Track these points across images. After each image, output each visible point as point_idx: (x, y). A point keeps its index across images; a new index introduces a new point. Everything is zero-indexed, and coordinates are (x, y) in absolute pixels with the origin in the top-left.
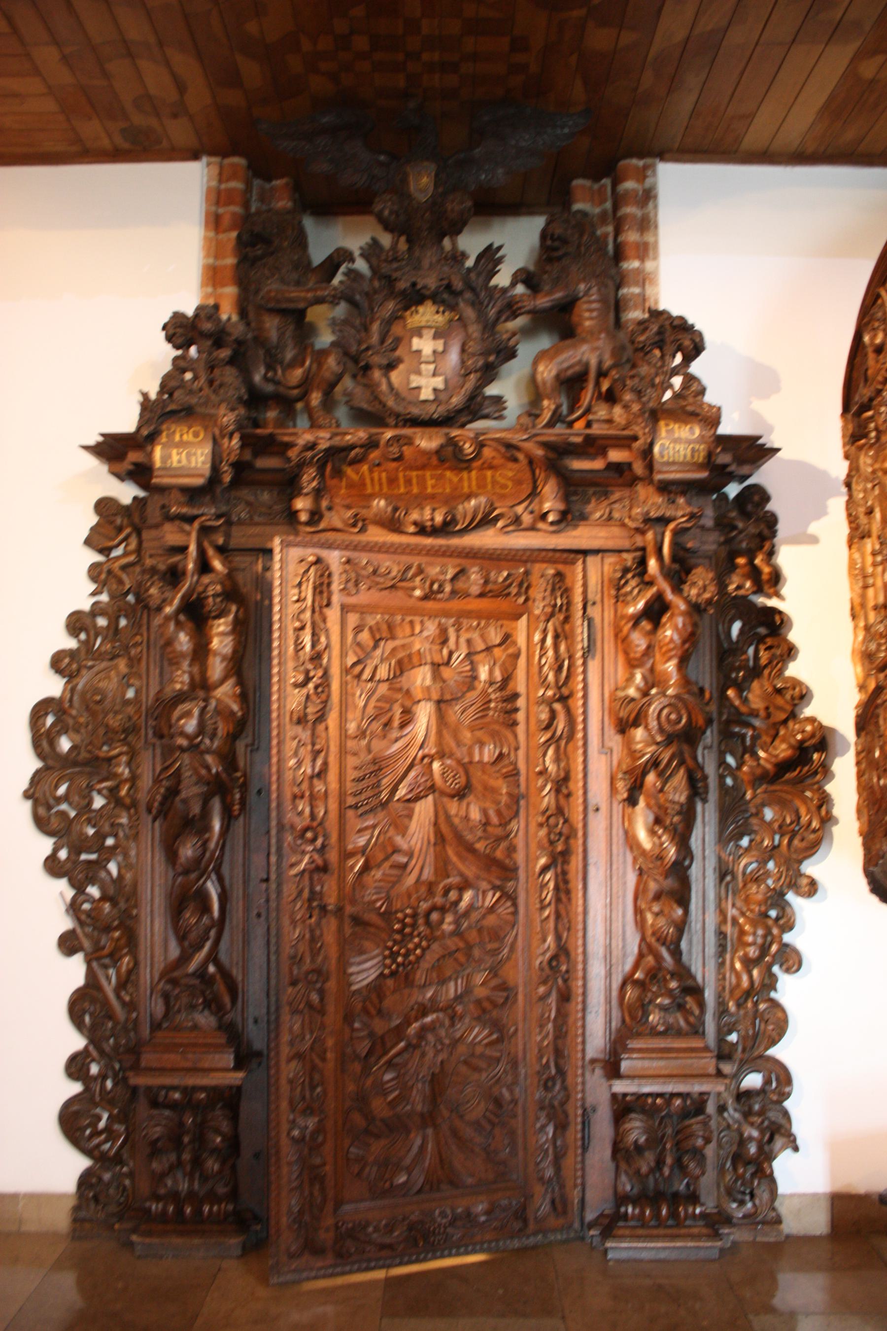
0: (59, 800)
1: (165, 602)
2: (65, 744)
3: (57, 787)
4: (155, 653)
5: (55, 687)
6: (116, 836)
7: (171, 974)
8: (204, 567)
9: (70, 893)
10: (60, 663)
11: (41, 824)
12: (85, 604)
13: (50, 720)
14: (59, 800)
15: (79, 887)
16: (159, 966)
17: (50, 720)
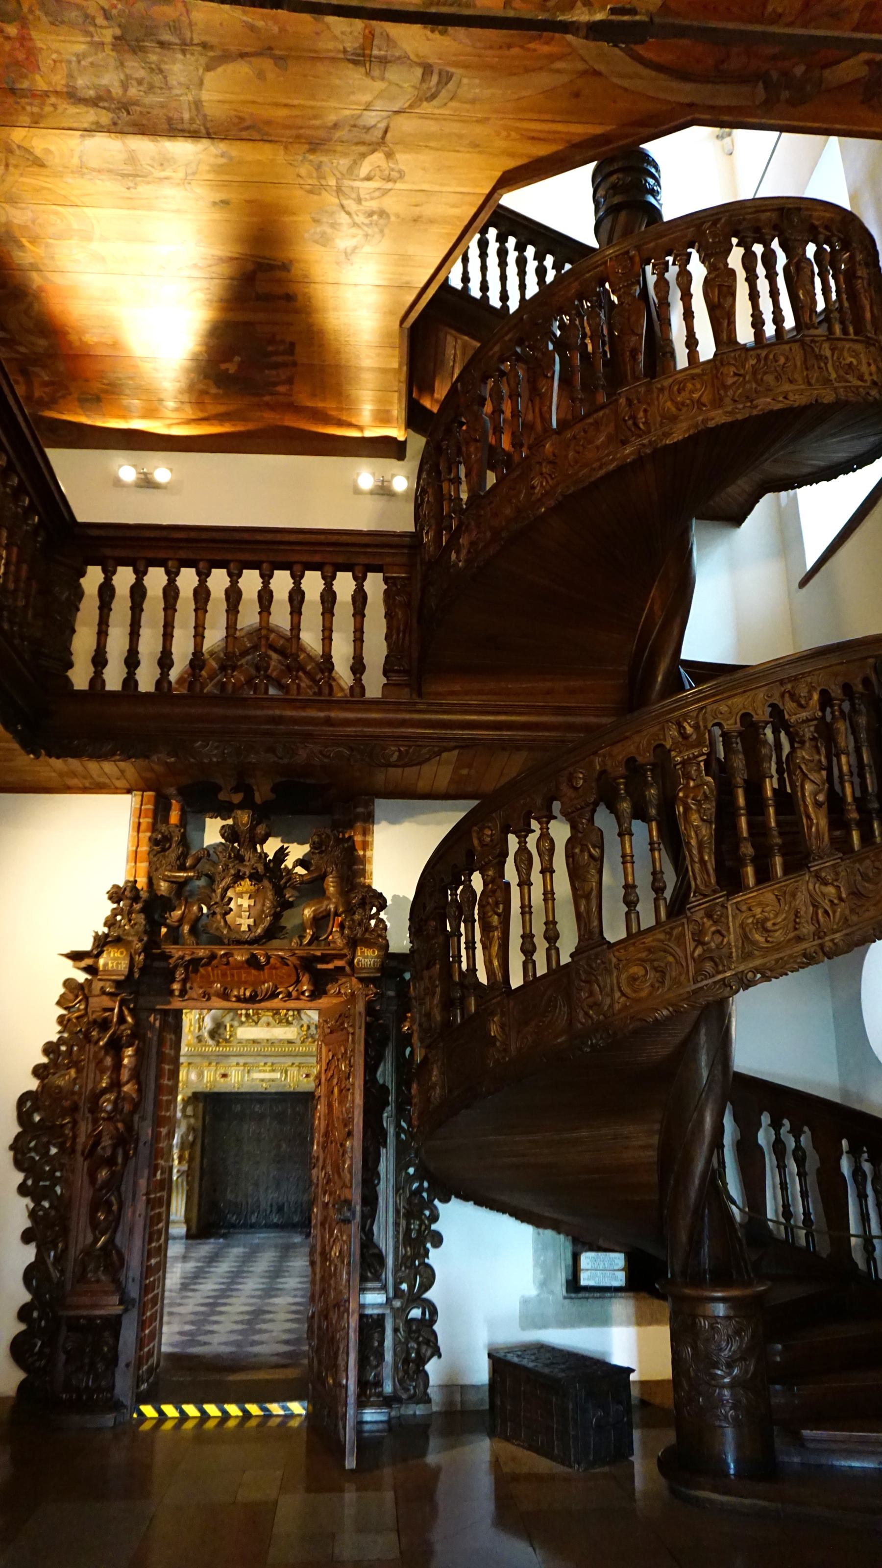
0: (30, 1150)
1: (99, 1039)
2: (37, 1118)
3: (30, 1142)
4: (92, 1066)
5: (33, 1084)
6: (61, 1171)
7: (88, 1252)
8: (122, 1019)
9: (31, 1205)
10: (39, 1071)
11: (18, 1164)
12: (54, 1038)
13: (29, 1104)
14: (30, 1150)
15: (37, 1201)
16: (80, 1247)
17: (29, 1104)
